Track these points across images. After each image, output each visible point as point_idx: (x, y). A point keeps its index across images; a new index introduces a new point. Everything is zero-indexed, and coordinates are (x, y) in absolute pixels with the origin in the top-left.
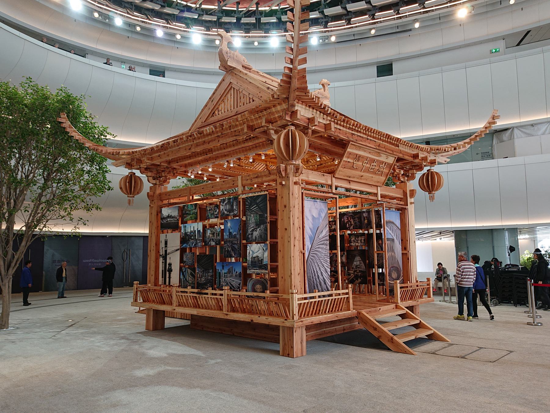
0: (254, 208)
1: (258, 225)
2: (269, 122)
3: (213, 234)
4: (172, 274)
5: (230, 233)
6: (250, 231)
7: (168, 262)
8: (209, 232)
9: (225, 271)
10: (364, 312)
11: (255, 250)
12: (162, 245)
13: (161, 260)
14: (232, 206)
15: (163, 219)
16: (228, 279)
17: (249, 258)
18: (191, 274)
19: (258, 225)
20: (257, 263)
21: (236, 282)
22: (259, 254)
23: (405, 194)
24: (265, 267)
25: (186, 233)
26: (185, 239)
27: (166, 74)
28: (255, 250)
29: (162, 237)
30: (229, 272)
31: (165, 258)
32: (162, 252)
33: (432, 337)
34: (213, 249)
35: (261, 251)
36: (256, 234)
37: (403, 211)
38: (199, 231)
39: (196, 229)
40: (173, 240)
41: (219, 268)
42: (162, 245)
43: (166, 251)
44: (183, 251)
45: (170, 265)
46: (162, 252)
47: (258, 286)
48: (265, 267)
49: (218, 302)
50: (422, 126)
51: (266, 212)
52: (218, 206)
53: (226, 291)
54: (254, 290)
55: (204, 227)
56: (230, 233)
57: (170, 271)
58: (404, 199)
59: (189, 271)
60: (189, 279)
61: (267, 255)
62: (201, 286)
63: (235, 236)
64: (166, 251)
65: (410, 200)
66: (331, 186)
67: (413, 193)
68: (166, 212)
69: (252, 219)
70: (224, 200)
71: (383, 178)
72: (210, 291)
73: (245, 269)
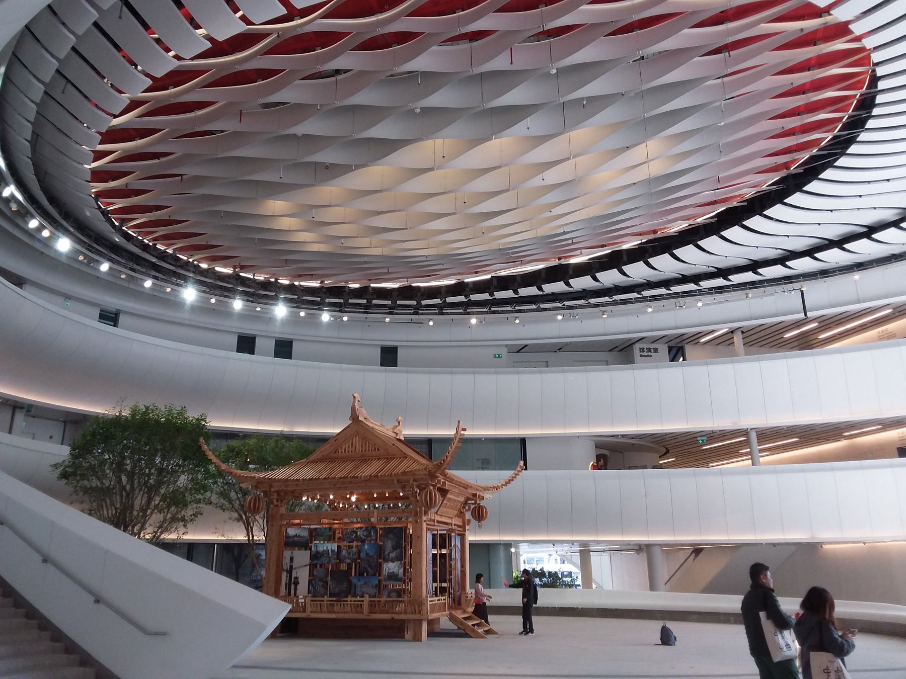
0: (391, 536)
1: (394, 548)
2: (415, 480)
3: (349, 554)
4: (299, 587)
5: (367, 554)
6: (386, 553)
7: (294, 575)
8: (344, 552)
9: (362, 582)
10: (453, 612)
11: (391, 567)
12: (287, 560)
13: (284, 575)
14: (370, 533)
15: (288, 537)
16: (364, 590)
17: (385, 572)
18: (323, 586)
19: (394, 548)
20: (392, 577)
21: (373, 591)
23: (464, 523)
24: (400, 580)
25: (317, 552)
26: (315, 556)
27: (122, 319)
28: (391, 567)
29: (287, 554)
30: (365, 583)
31: (290, 572)
32: (286, 566)
33: (488, 632)
34: (350, 565)
35: (397, 568)
36: (393, 555)
37: (463, 537)
38: (333, 551)
39: (329, 548)
40: (302, 557)
41: (354, 580)
42: (287, 560)
43: (291, 567)
44: (312, 567)
45: (296, 578)
46: (286, 566)
47: (394, 594)
48: (400, 580)
49: (359, 605)
50: (428, 426)
51: (401, 540)
52: (356, 532)
53: (367, 599)
54: (389, 597)
55: (339, 547)
56: (367, 554)
57: (296, 583)
58: (463, 527)
59: (320, 584)
60: (321, 590)
61: (402, 570)
62: (339, 596)
63: (372, 556)
64: (291, 567)
65: (467, 527)
66: (434, 521)
67: (469, 521)
68: (292, 532)
69: (389, 545)
70: (361, 528)
71: (456, 512)
72: (349, 598)
73: (380, 581)
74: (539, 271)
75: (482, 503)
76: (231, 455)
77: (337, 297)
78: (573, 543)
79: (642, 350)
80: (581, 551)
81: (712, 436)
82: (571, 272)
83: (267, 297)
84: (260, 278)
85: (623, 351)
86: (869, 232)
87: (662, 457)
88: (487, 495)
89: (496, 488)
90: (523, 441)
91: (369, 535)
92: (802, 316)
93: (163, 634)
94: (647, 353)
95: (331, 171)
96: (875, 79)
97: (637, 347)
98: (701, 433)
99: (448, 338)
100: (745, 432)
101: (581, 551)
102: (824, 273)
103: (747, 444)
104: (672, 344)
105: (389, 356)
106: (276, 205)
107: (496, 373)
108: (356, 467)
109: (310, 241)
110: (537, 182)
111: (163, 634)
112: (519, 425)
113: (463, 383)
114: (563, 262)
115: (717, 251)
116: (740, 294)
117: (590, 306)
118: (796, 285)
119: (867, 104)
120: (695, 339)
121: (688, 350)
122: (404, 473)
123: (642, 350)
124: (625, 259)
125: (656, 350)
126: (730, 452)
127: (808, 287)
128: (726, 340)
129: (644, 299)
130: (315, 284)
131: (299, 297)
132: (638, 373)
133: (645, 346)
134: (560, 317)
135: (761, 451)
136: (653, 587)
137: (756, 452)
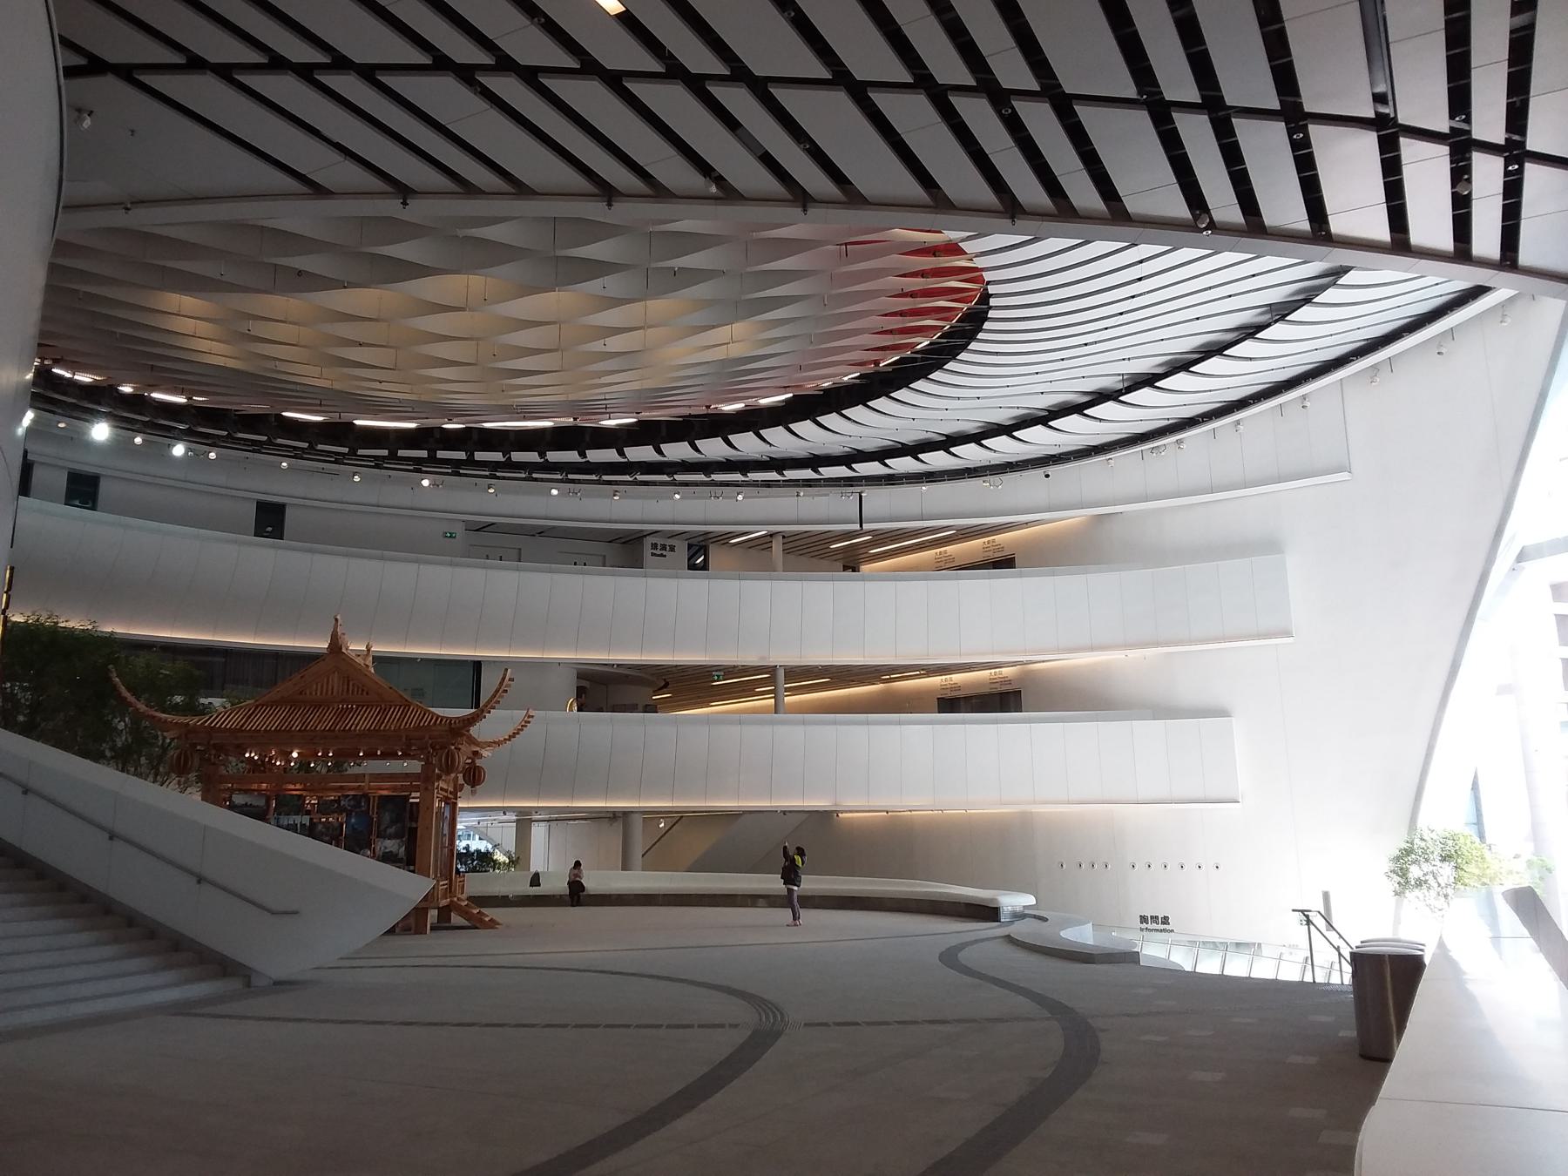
1: (393, 822)
19: (393, 822)
22: (394, 849)
36: (391, 830)
69: (387, 817)
74: (544, 430)
75: (478, 762)
76: (155, 690)
77: (202, 423)
78: (505, 810)
79: (654, 546)
80: (517, 821)
81: (731, 671)
82: (587, 438)
83: (75, 407)
84: (84, 378)
85: (628, 549)
86: (948, 443)
87: (658, 691)
88: (485, 753)
89: (498, 743)
90: (477, 665)
91: (358, 805)
92: (857, 527)
93: (296, 913)
94: (662, 550)
95: (303, 281)
96: (986, 297)
97: (649, 541)
98: (718, 668)
99: (374, 501)
100: (772, 670)
101: (517, 821)
102: (891, 480)
103: (772, 680)
104: (694, 541)
105: (270, 520)
106: (187, 302)
107: (451, 564)
108: (342, 714)
109: (216, 352)
110: (597, 346)
111: (296, 913)
112: (476, 642)
113: (399, 576)
114: (579, 423)
115: (779, 441)
116: (794, 490)
117: (599, 482)
118: (858, 489)
119: (974, 321)
120: (723, 539)
121: (714, 551)
122: (418, 728)
123: (654, 546)
124: (664, 432)
125: (672, 549)
126: (745, 691)
127: (869, 493)
128: (764, 543)
129: (674, 483)
130: (181, 400)
131: (134, 413)
132: (651, 581)
133: (659, 541)
134: (554, 492)
135: (787, 690)
136: (626, 866)
137: (781, 691)
